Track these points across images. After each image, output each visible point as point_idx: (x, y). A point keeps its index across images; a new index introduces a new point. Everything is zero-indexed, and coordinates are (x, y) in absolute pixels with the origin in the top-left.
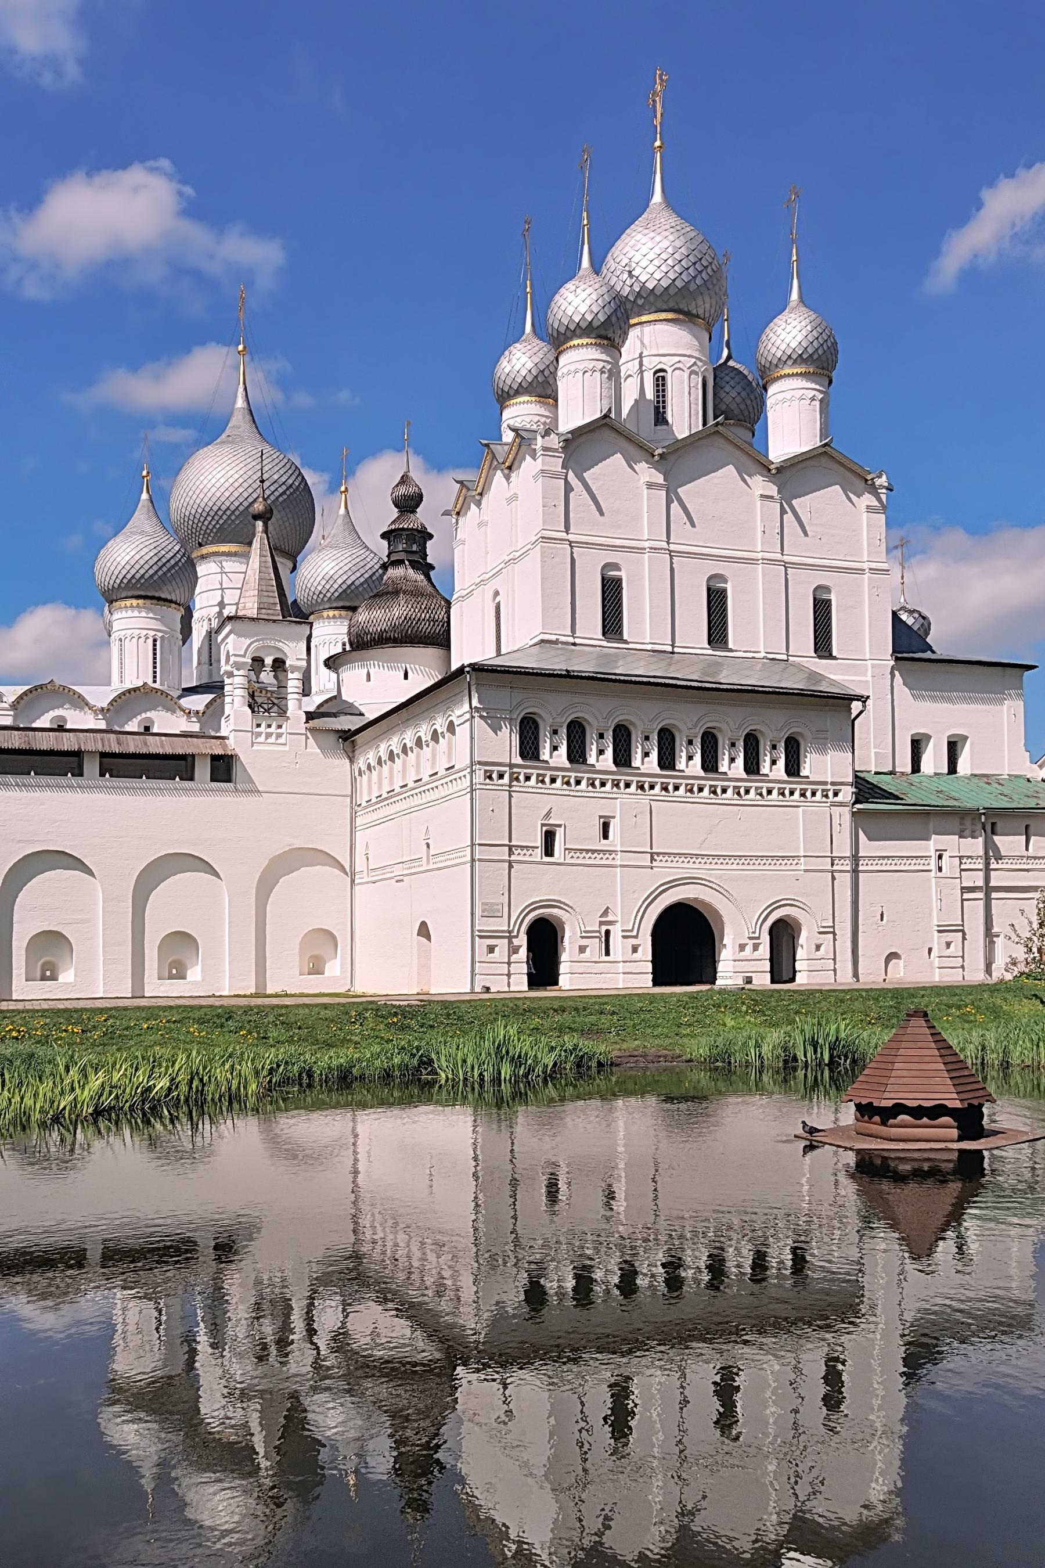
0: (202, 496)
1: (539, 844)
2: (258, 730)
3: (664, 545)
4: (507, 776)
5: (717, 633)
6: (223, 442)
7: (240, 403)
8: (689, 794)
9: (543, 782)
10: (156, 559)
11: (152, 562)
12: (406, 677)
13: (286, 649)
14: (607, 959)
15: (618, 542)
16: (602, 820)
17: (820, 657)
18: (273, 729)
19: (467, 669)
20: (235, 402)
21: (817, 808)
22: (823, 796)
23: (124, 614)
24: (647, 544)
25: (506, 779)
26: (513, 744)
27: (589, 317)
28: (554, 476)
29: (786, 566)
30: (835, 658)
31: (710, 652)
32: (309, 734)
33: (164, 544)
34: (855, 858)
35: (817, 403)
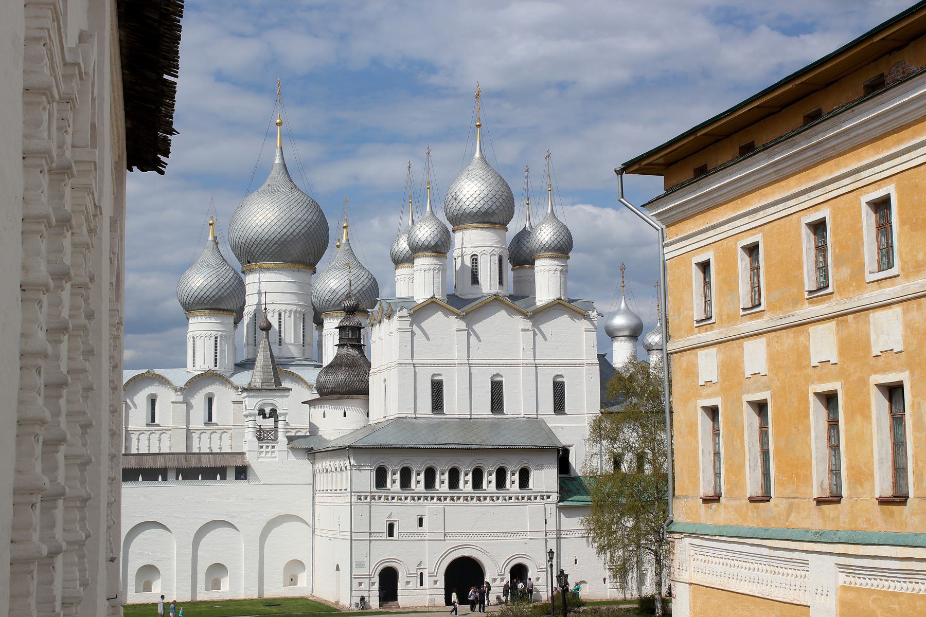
0: (249, 231)
1: (385, 531)
2: (261, 450)
3: (466, 361)
4: (369, 497)
5: (497, 403)
6: (265, 192)
7: (277, 160)
8: (465, 501)
9: (387, 499)
10: (217, 284)
11: (214, 287)
12: (345, 416)
13: (277, 405)
14: (421, 587)
15: (440, 362)
16: (418, 517)
17: (556, 414)
18: (269, 449)
19: (347, 448)
20: (274, 160)
21: (537, 506)
22: (541, 499)
23: (199, 320)
24: (457, 362)
25: (368, 500)
26: (372, 482)
27: (426, 243)
28: (405, 331)
29: (536, 366)
30: (566, 414)
31: (493, 416)
32: (289, 450)
33: (223, 273)
34: (559, 531)
35: (559, 273)
